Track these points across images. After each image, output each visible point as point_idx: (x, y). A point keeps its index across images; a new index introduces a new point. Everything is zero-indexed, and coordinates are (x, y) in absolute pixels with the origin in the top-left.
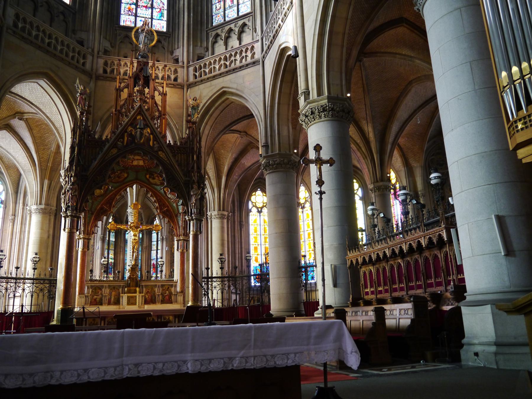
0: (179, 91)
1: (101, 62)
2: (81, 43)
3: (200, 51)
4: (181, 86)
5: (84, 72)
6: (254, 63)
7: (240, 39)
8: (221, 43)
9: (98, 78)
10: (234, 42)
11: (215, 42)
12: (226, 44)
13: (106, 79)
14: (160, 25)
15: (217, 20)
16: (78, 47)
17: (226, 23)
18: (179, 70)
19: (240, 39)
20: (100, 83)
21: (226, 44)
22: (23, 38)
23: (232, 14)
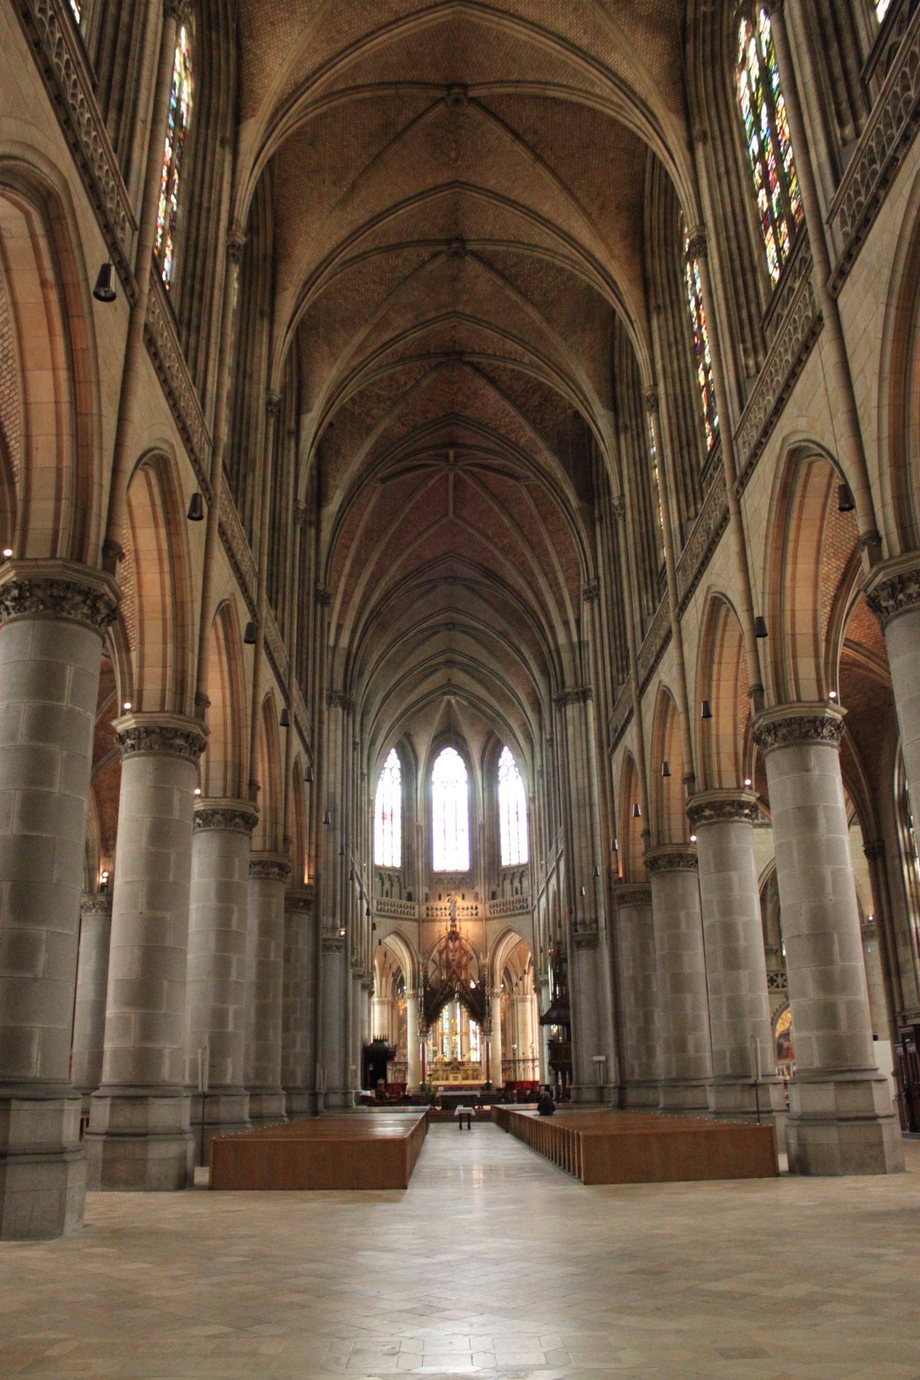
0: (479, 923)
1: (424, 908)
2: (410, 898)
3: (493, 887)
4: (481, 920)
5: (415, 920)
6: (527, 913)
7: (521, 882)
8: (508, 882)
9: (424, 921)
10: (516, 884)
11: (504, 879)
12: (512, 883)
13: (428, 921)
14: (463, 865)
15: (505, 862)
16: (410, 904)
17: (509, 868)
18: (479, 907)
19: (521, 882)
20: (426, 924)
21: (512, 883)
22: (382, 916)
23: (514, 862)
